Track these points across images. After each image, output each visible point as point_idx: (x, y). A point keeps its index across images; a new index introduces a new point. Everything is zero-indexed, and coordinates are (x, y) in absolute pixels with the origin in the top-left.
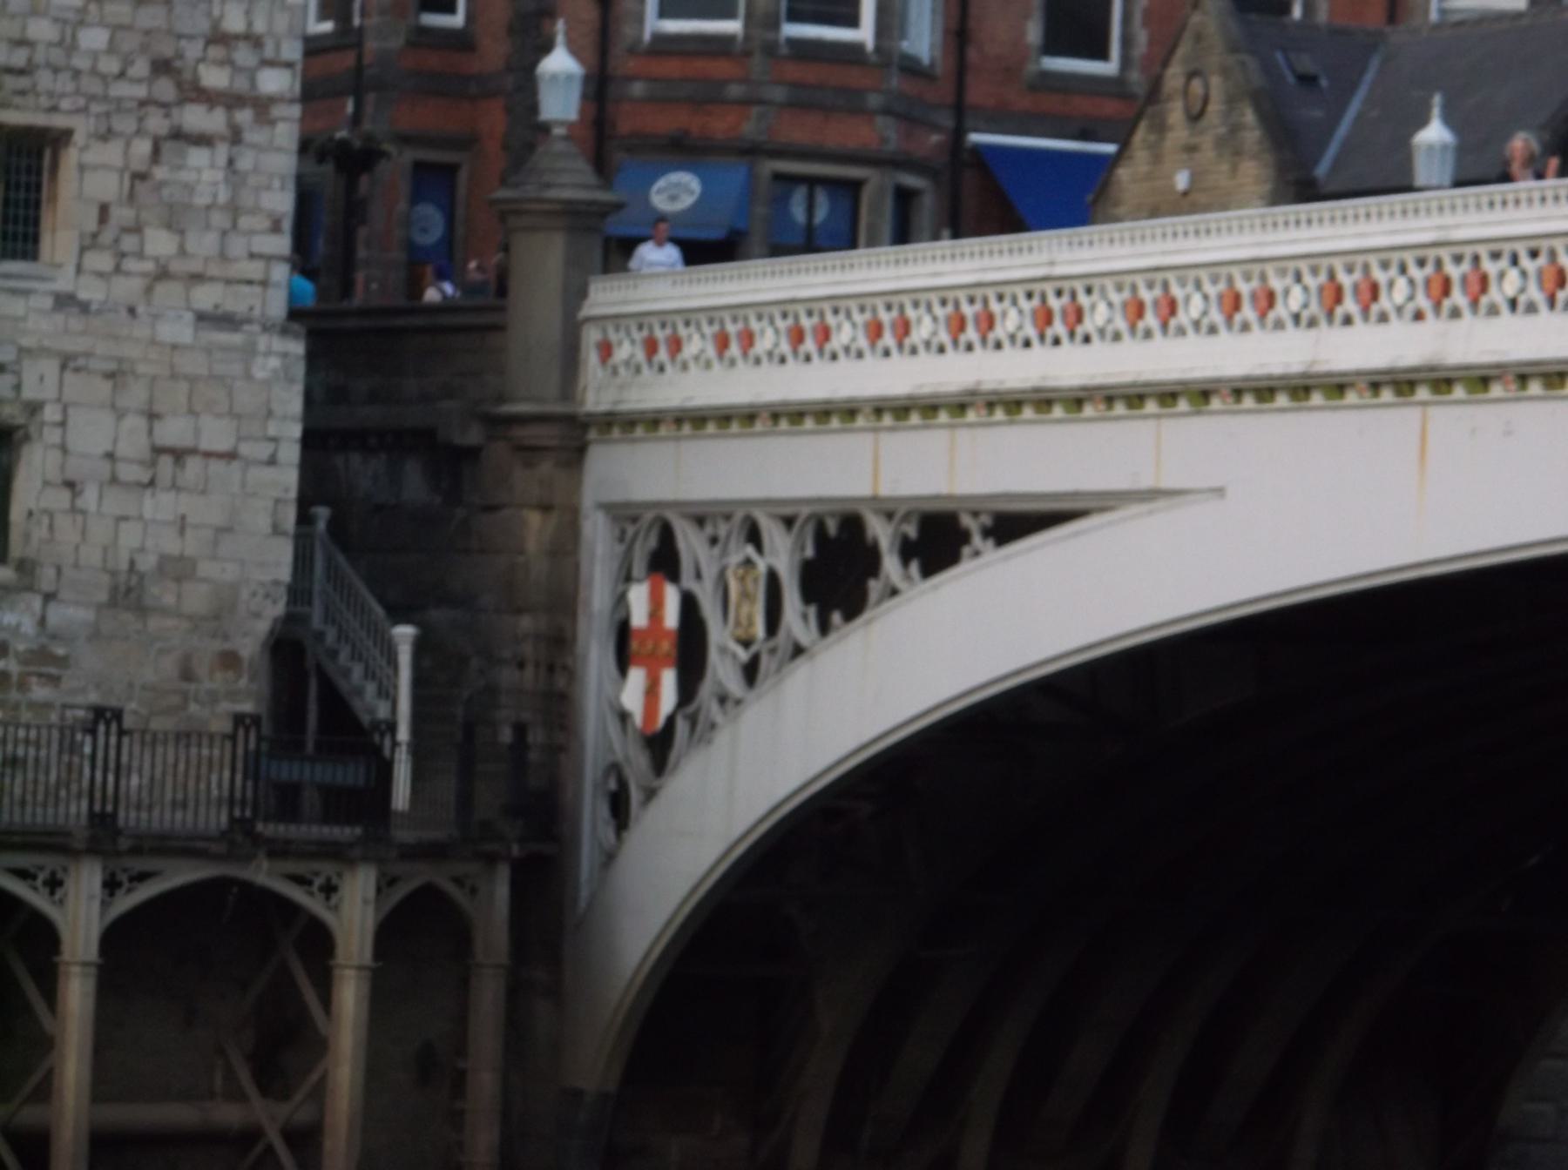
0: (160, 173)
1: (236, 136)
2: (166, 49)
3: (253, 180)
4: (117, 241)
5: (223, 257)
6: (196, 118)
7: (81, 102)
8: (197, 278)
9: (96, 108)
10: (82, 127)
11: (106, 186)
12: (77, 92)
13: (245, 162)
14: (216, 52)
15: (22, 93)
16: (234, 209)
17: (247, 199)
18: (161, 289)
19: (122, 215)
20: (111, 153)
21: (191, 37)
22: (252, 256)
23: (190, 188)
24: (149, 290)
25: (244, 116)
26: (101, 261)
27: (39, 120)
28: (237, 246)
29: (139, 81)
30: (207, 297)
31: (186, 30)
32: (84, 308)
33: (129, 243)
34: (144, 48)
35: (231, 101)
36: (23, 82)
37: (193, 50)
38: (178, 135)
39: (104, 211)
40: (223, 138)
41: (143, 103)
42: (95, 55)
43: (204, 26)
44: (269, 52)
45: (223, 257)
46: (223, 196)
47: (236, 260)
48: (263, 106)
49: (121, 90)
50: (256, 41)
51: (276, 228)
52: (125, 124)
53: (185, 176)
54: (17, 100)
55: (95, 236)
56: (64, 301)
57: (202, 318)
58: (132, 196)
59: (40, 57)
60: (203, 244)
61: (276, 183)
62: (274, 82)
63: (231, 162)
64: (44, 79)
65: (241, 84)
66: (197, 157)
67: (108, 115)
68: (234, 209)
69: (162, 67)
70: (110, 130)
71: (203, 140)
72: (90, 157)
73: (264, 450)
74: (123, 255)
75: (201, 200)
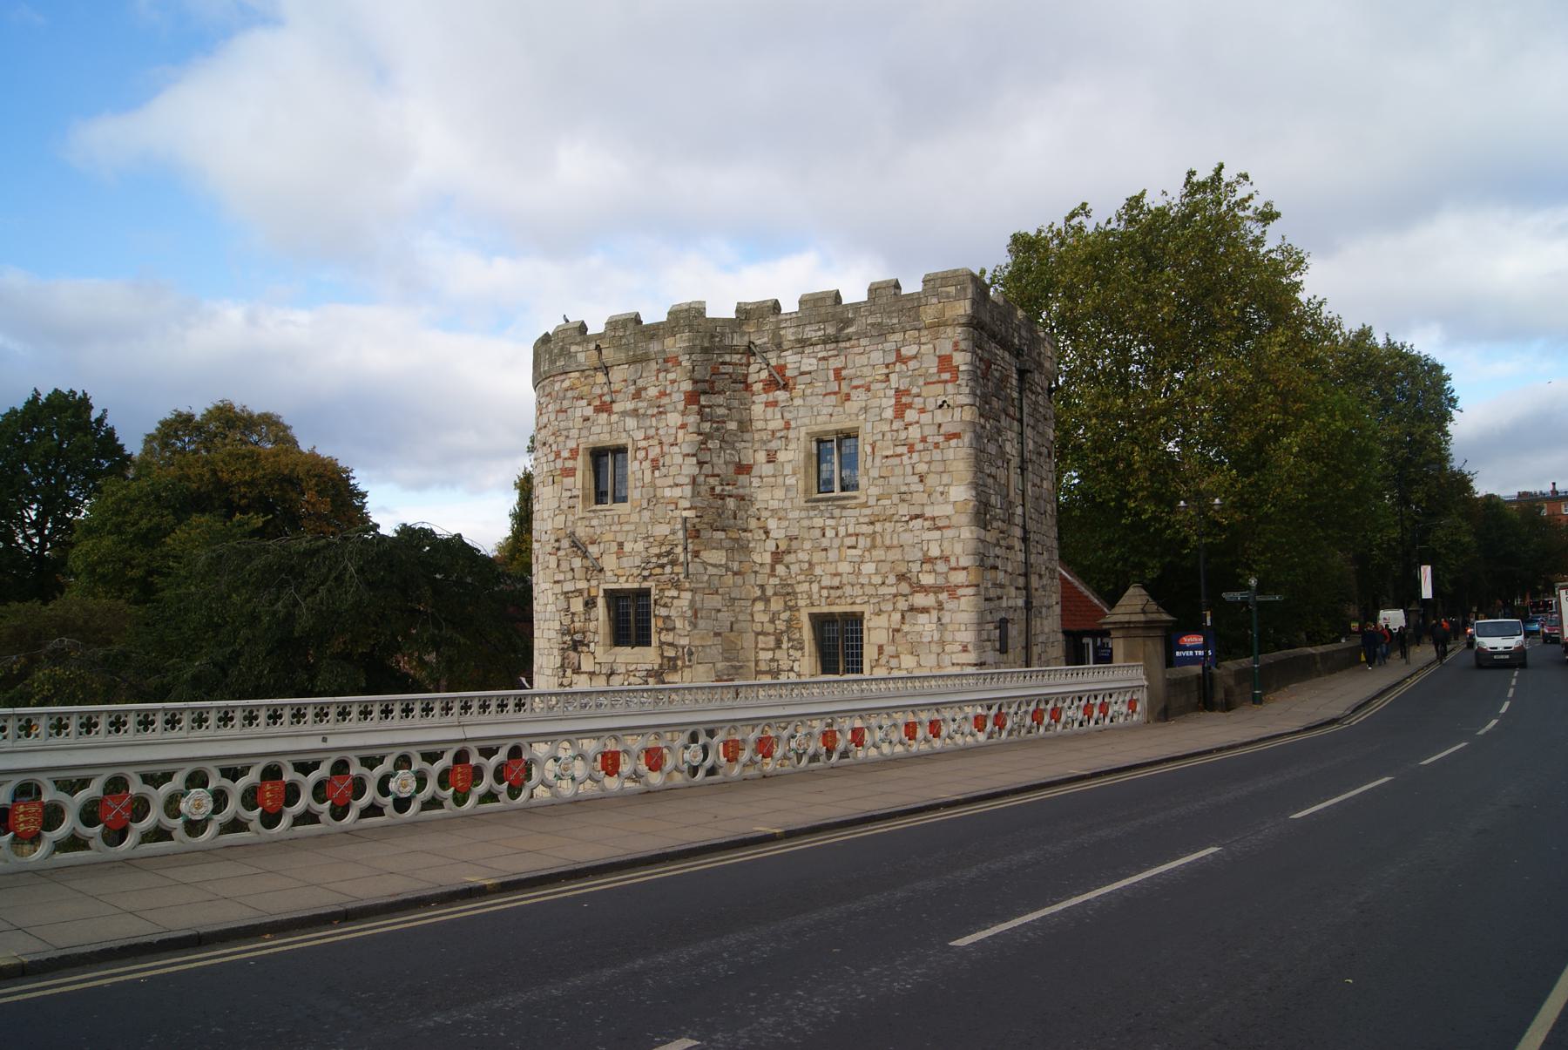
0: (906, 628)
1: (940, 607)
3: (950, 627)
4: (888, 662)
6: (920, 600)
7: (866, 599)
9: (872, 601)
10: (868, 610)
12: (864, 594)
13: (945, 620)
14: (926, 567)
15: (839, 597)
16: (942, 643)
17: (948, 637)
19: (889, 650)
20: (882, 621)
21: (914, 562)
22: (953, 664)
23: (920, 634)
25: (944, 596)
27: (848, 609)
28: (946, 659)
29: (892, 585)
31: (911, 559)
33: (894, 662)
34: (892, 570)
35: (937, 589)
36: (839, 592)
37: (915, 567)
38: (912, 609)
39: (881, 648)
40: (934, 609)
41: (895, 596)
42: (869, 576)
43: (920, 555)
44: (953, 563)
46: (936, 637)
47: (946, 667)
48: (952, 590)
49: (883, 590)
50: (946, 559)
51: (965, 649)
52: (888, 607)
53: (917, 628)
54: (837, 601)
55: (877, 660)
58: (893, 640)
59: (845, 581)
61: (963, 628)
62: (959, 578)
63: (939, 619)
64: (848, 590)
65: (941, 581)
66: (923, 618)
67: (879, 603)
68: (942, 643)
69: (902, 577)
70: (880, 610)
71: (925, 610)
72: (872, 624)
74: (892, 669)
75: (925, 640)
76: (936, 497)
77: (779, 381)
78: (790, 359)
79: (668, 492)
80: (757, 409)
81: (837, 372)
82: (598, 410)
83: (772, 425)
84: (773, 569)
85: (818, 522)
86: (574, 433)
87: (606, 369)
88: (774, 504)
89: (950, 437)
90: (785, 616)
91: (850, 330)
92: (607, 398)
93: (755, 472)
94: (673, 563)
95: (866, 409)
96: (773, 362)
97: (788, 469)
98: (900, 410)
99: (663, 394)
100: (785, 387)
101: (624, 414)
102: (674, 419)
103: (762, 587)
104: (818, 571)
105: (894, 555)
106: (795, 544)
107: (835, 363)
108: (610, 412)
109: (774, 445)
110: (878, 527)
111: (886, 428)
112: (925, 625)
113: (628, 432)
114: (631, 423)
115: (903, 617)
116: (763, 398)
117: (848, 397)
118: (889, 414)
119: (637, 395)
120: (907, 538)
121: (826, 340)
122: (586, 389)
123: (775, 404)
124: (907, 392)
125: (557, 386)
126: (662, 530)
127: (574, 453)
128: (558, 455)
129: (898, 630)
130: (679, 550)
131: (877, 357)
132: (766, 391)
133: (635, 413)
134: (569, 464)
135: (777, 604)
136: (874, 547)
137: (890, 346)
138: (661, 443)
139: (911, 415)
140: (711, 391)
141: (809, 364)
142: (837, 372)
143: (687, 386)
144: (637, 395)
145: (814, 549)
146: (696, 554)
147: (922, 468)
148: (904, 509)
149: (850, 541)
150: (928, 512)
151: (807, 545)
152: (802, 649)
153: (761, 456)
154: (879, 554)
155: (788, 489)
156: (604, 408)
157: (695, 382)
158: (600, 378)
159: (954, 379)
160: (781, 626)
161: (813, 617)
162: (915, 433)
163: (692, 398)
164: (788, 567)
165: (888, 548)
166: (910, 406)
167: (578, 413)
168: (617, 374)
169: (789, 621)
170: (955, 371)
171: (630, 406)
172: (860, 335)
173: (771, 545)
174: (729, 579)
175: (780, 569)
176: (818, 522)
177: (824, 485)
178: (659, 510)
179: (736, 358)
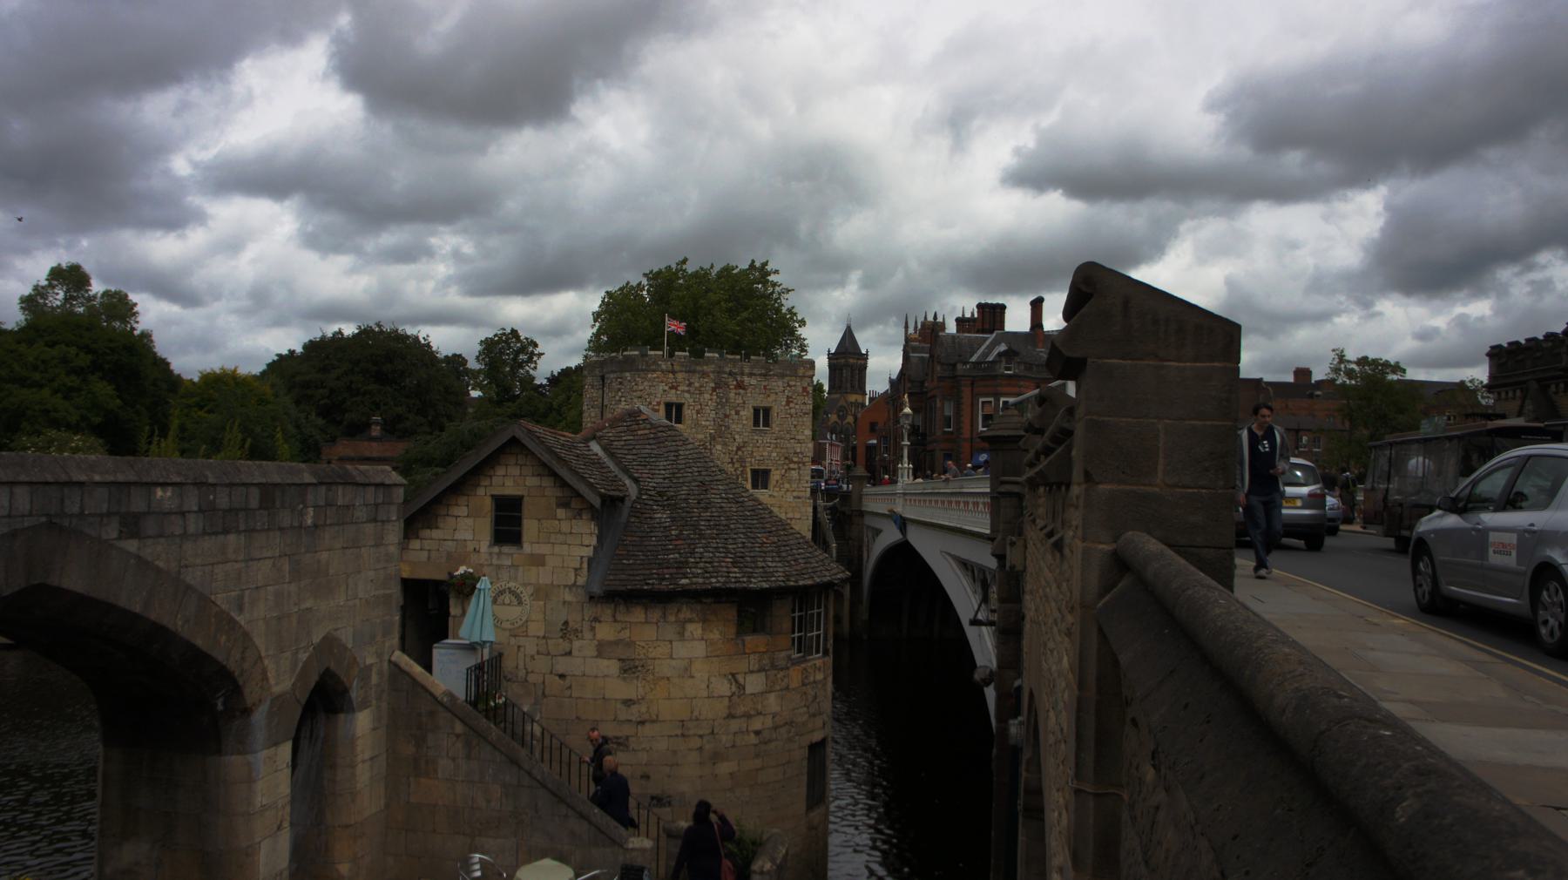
1: (799, 468)
2: (787, 455)
5: (798, 487)
6: (792, 466)
8: (794, 491)
10: (773, 468)
11: (778, 477)
13: (801, 472)
16: (800, 480)
18: (789, 494)
19: (780, 481)
20: (778, 472)
24: (785, 494)
25: (801, 465)
26: (778, 489)
28: (800, 485)
30: (795, 494)
32: (774, 497)
38: (789, 469)
39: (777, 481)
43: (792, 451)
45: (798, 487)
50: (802, 453)
56: (770, 496)
57: (795, 497)
60: (794, 486)
66: (793, 472)
68: (800, 480)
69: (786, 458)
73: (805, 518)
76: (800, 433)
77: (740, 386)
78: (746, 379)
79: (703, 423)
80: (732, 395)
81: (765, 386)
82: (671, 388)
83: (737, 402)
84: (736, 452)
85: (756, 438)
86: (659, 395)
87: (674, 372)
88: (738, 430)
89: (805, 414)
90: (740, 469)
91: (771, 373)
92: (674, 384)
93: (731, 417)
94: (705, 449)
95: (775, 401)
96: (739, 379)
97: (744, 418)
98: (788, 403)
99: (701, 386)
100: (744, 389)
101: (683, 391)
102: (707, 396)
103: (732, 459)
104: (755, 454)
105: (783, 451)
106: (746, 444)
107: (764, 383)
108: (676, 389)
109: (738, 408)
110: (778, 441)
111: (782, 408)
112: (794, 474)
113: (687, 399)
114: (687, 395)
115: (786, 471)
116: (734, 391)
117: (769, 396)
118: (784, 403)
119: (690, 385)
120: (789, 445)
121: (760, 375)
122: (665, 379)
123: (739, 394)
124: (791, 397)
125: (650, 376)
126: (701, 436)
127: (659, 404)
128: (650, 403)
129: (783, 476)
130: (708, 444)
131: (780, 383)
132: (735, 388)
133: (688, 392)
134: (657, 407)
135: (736, 466)
136: (777, 447)
137: (785, 381)
138: (701, 405)
139: (792, 405)
140: (719, 388)
141: (753, 382)
142: (765, 386)
143: (713, 385)
144: (690, 385)
145: (753, 447)
146: (714, 446)
147: (795, 423)
148: (788, 436)
149: (768, 445)
150: (797, 437)
151: (751, 445)
152: (747, 481)
153: (733, 412)
154: (778, 450)
155: (744, 425)
156: (675, 388)
157: (715, 384)
158: (671, 375)
159: (807, 395)
160: (739, 472)
161: (751, 470)
162: (793, 411)
163: (714, 390)
164: (743, 452)
165: (782, 448)
166: (792, 402)
167: (661, 388)
168: (680, 376)
169: (742, 471)
170: (808, 392)
171: (687, 389)
172: (774, 375)
173: (736, 444)
174: (722, 455)
175: (740, 453)
176: (756, 438)
177: (756, 423)
178: (700, 429)
179: (726, 376)
